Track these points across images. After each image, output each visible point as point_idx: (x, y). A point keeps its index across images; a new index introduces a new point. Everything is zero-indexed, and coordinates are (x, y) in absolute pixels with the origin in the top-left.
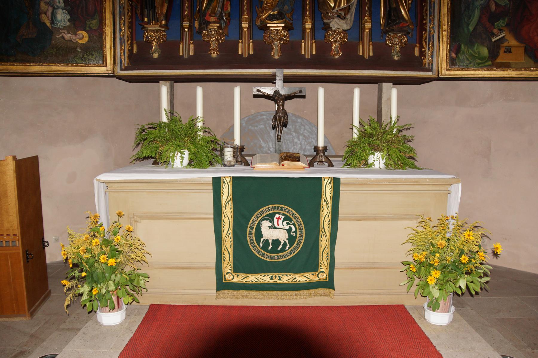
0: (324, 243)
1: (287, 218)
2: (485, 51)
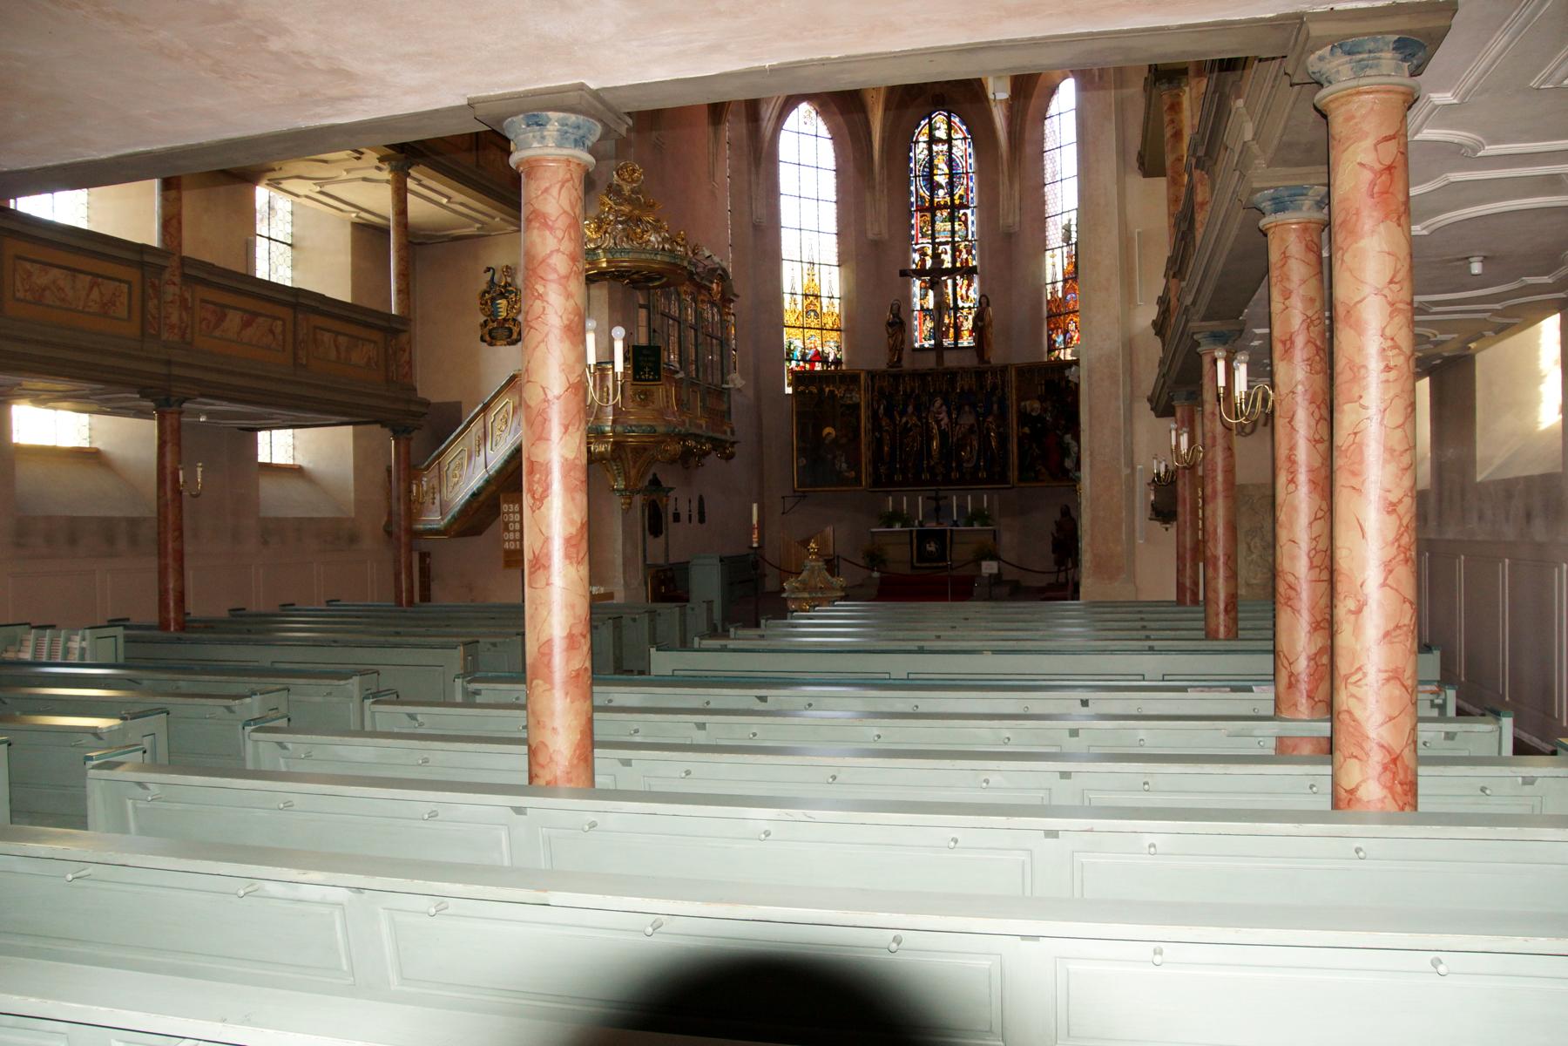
0: (948, 552)
1: (936, 544)
2: (1033, 475)
